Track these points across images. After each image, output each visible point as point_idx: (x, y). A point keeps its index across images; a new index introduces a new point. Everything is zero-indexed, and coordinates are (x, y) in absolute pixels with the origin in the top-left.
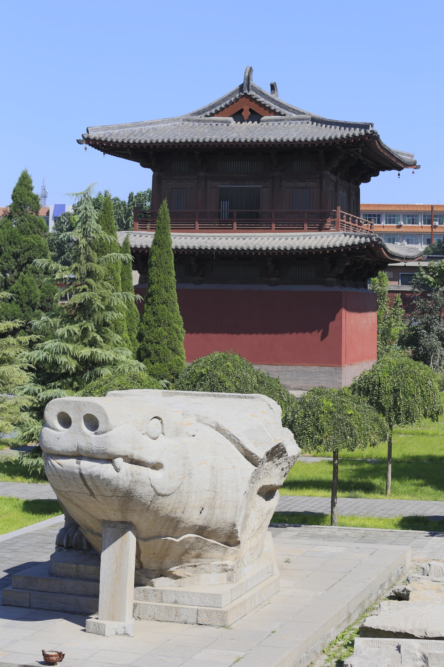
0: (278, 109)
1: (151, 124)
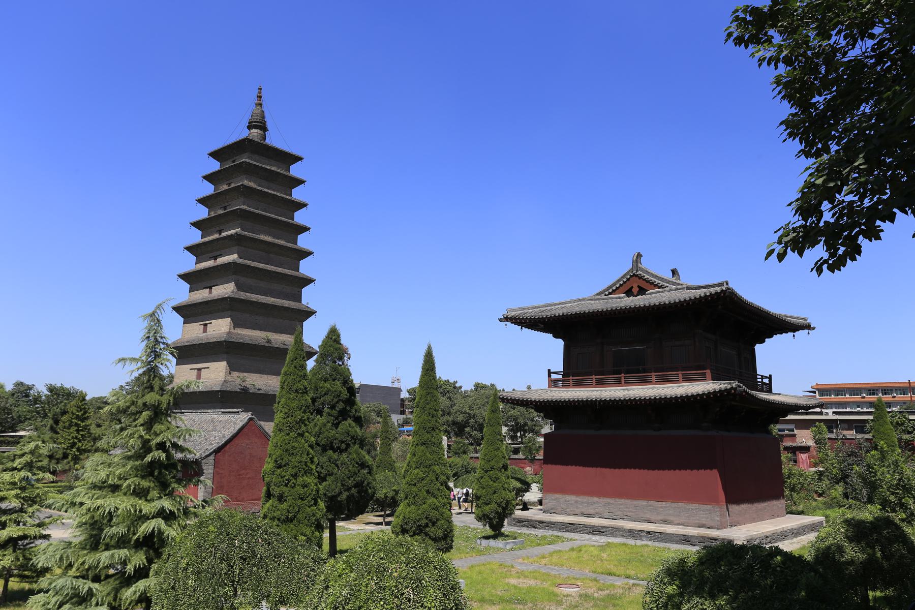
0: (662, 283)
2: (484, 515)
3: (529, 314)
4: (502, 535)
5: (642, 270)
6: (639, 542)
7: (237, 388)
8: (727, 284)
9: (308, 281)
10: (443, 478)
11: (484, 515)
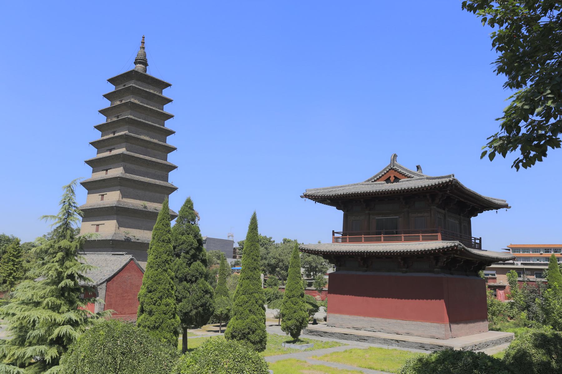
0: (410, 175)
1: (341, 187)
2: (287, 327)
3: (321, 193)
4: (299, 340)
5: (397, 166)
6: (391, 347)
7: (123, 238)
8: (453, 176)
9: (173, 168)
10: (260, 302)
11: (287, 327)
